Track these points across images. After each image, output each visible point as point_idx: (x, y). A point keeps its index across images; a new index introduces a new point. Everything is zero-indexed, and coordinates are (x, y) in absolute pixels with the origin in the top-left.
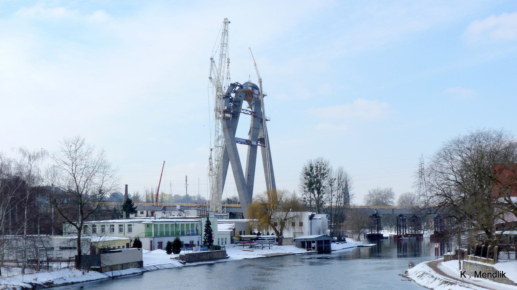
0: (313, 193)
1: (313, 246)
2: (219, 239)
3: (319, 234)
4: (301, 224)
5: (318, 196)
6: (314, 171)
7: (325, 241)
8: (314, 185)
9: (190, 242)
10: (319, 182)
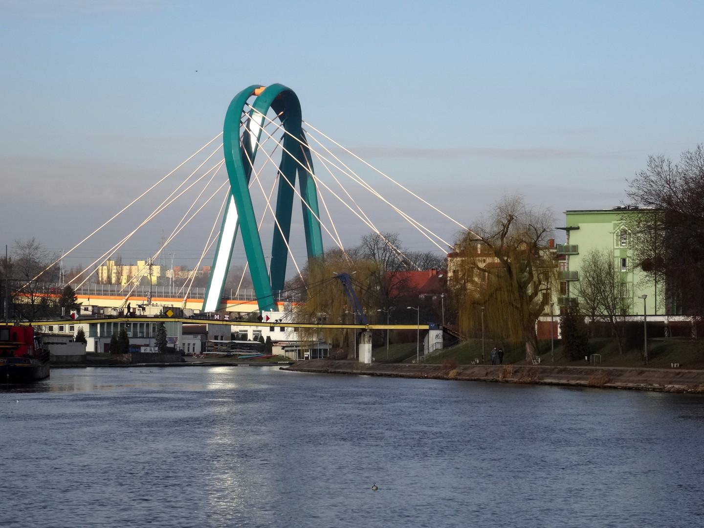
1: (306, 356)
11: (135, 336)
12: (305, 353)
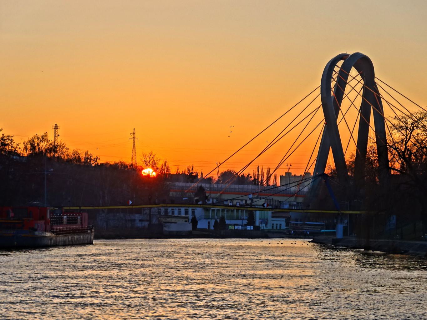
2: (273, 224)
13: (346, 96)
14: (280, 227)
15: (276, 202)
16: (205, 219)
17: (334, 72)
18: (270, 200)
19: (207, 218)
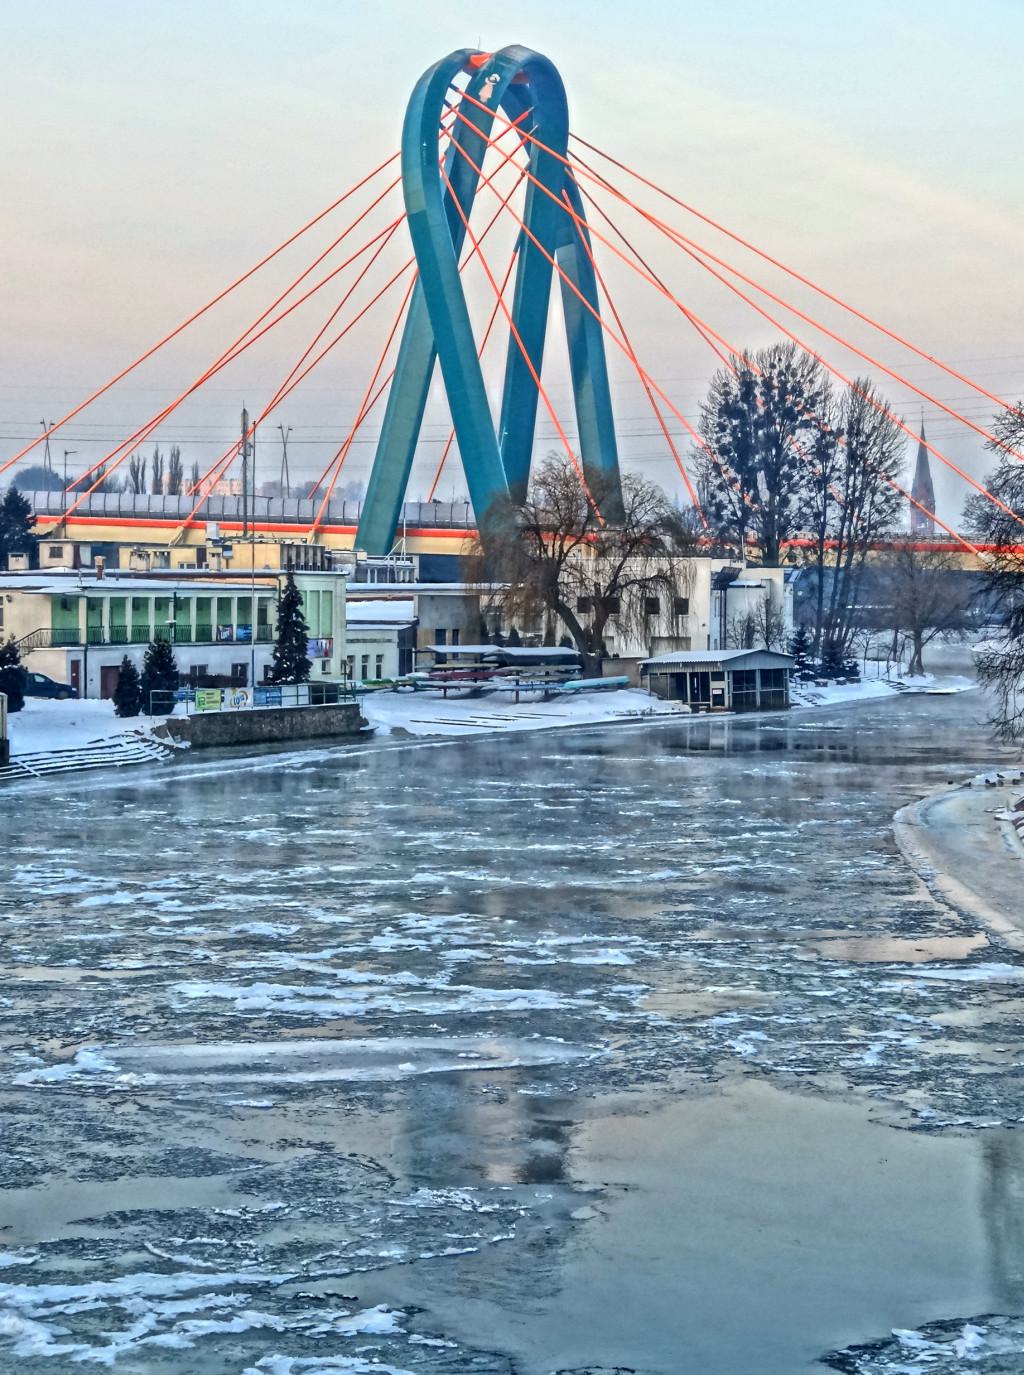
0: (749, 483)
1: (716, 692)
2: (351, 658)
3: (749, 647)
4: (681, 607)
5: (772, 498)
6: (760, 399)
7: (763, 672)
8: (758, 457)
9: (235, 667)
10: (774, 441)
11: (204, 636)
12: (713, 684)
13: (487, 181)
14: (379, 675)
15: (315, 554)
16: (53, 645)
17: (444, 106)
18: (298, 547)
19: (64, 638)
